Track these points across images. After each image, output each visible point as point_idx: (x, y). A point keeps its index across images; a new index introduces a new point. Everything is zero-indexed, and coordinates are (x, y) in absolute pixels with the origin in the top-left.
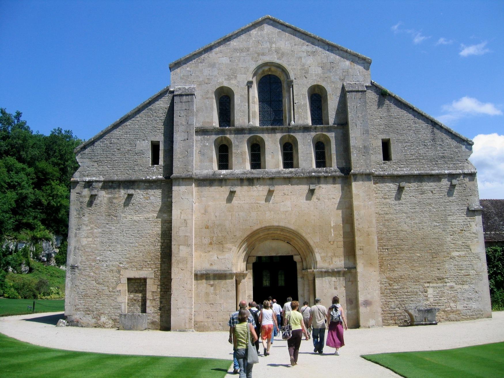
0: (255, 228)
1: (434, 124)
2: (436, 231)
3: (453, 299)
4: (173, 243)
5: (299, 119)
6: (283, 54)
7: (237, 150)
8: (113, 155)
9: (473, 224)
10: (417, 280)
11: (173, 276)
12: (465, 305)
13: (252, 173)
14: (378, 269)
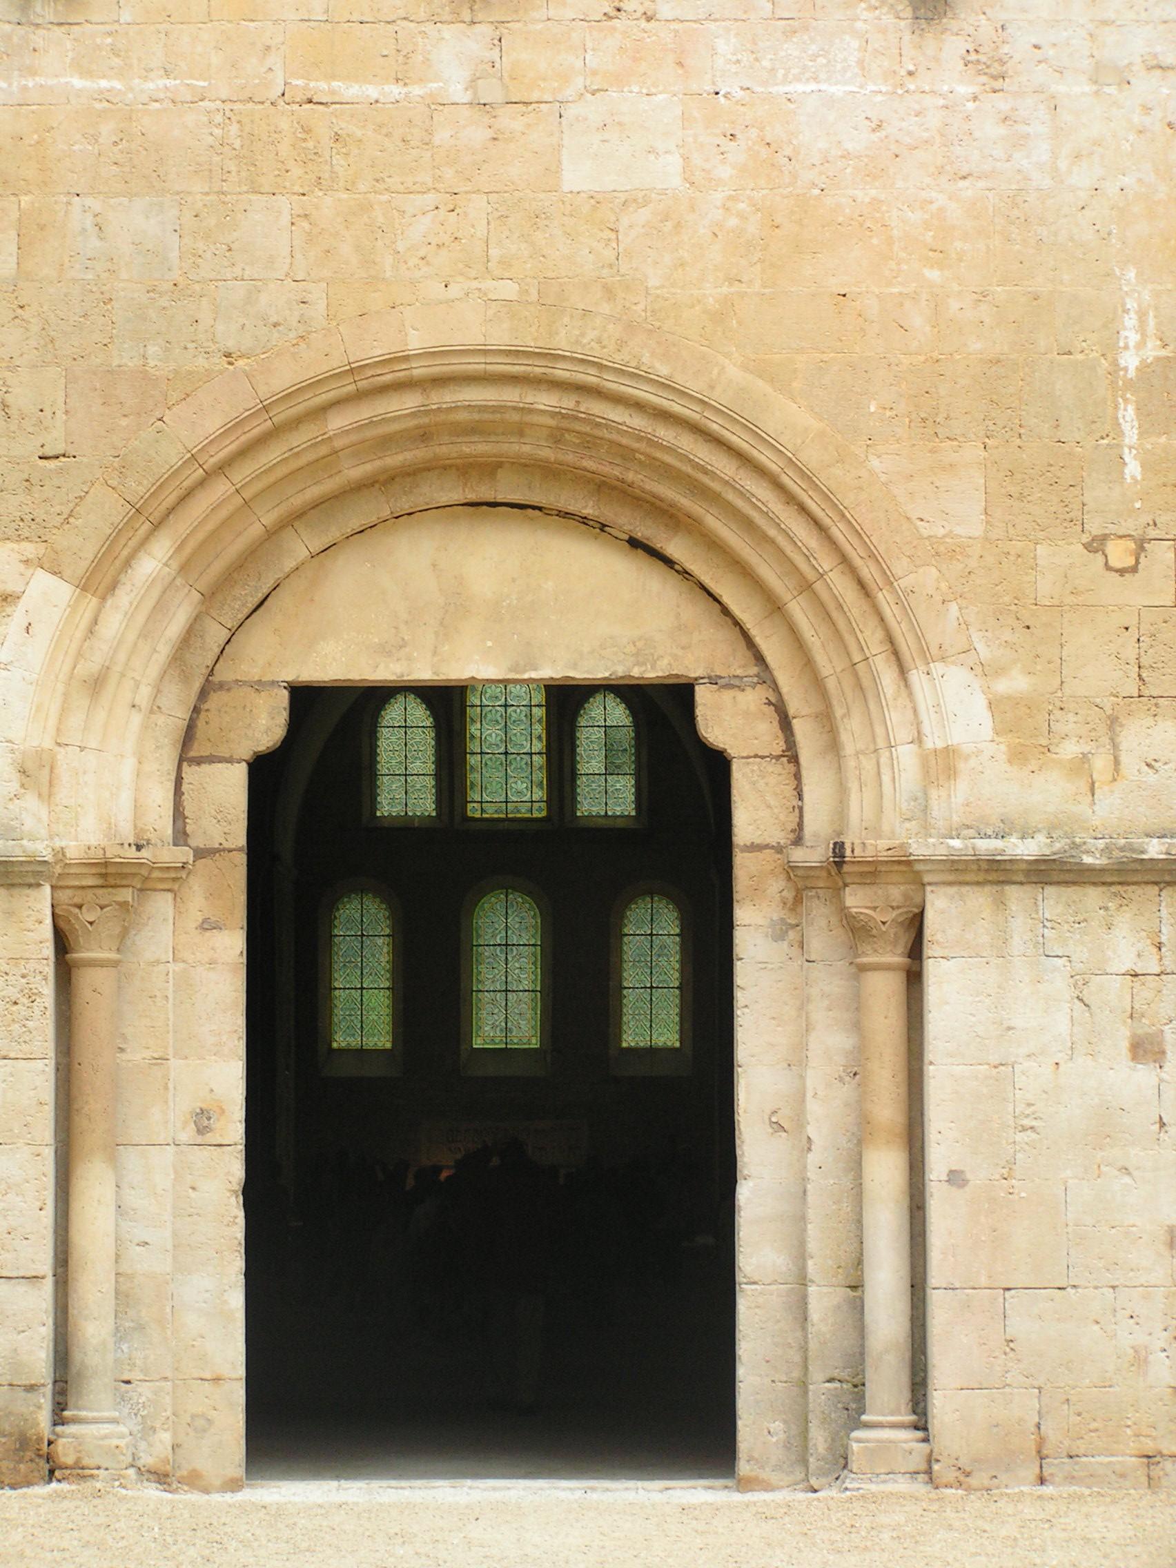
0: (284, 377)
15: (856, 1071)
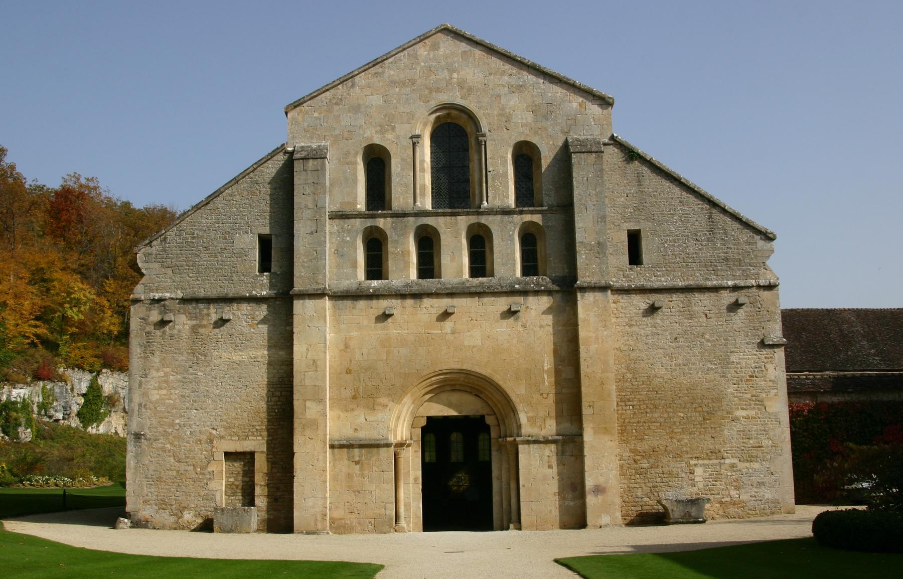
1: (713, 204)
2: (711, 376)
3: (734, 484)
4: (295, 397)
5: (494, 198)
6: (470, 90)
7: (396, 248)
8: (198, 256)
9: (770, 367)
10: (678, 456)
11: (296, 449)
12: (753, 494)
13: (420, 285)
14: (616, 436)
15: (509, 470)
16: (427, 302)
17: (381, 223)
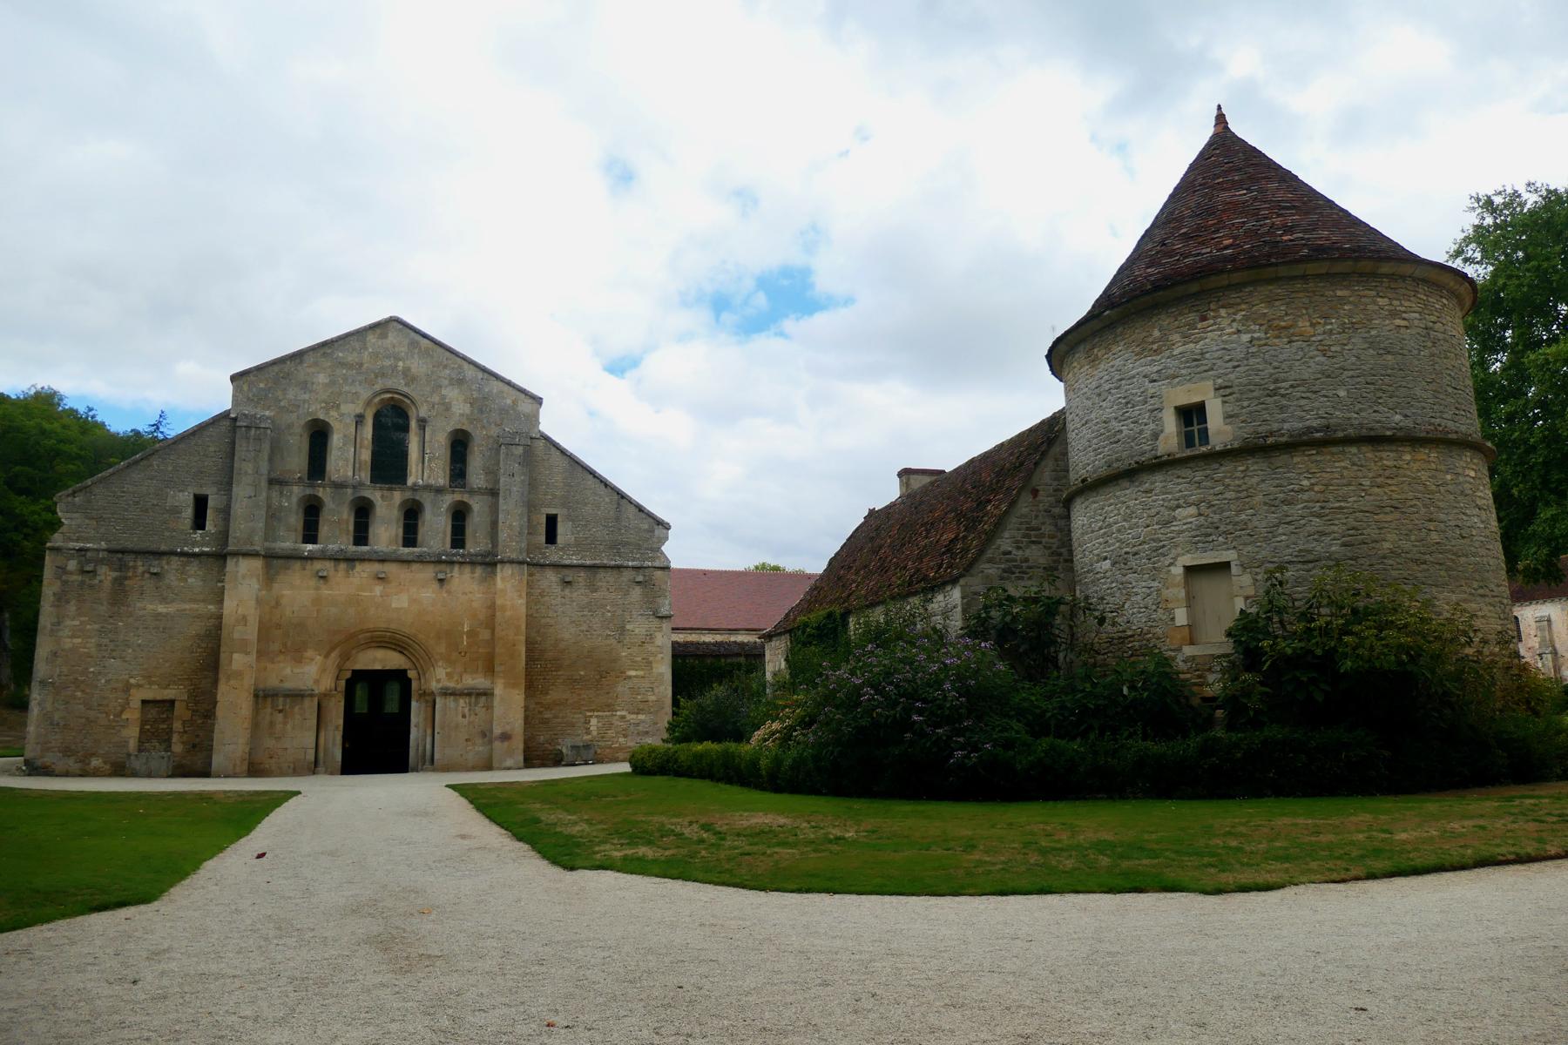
9: (659, 635)
16: (359, 567)
17: (320, 493)
